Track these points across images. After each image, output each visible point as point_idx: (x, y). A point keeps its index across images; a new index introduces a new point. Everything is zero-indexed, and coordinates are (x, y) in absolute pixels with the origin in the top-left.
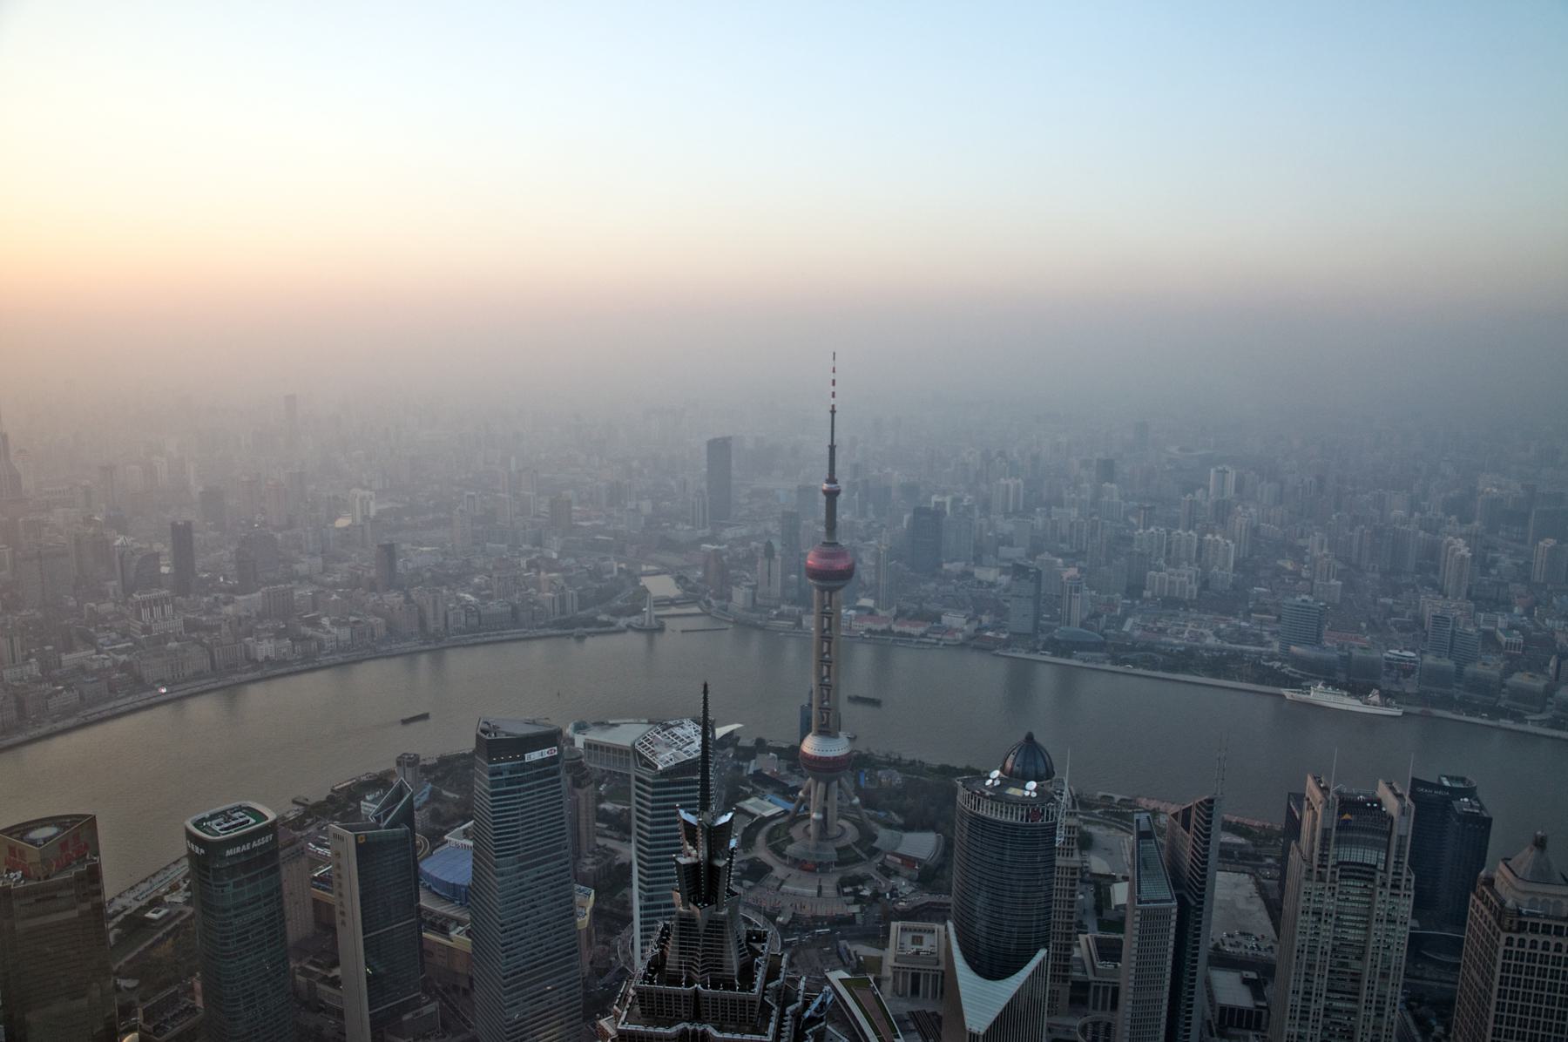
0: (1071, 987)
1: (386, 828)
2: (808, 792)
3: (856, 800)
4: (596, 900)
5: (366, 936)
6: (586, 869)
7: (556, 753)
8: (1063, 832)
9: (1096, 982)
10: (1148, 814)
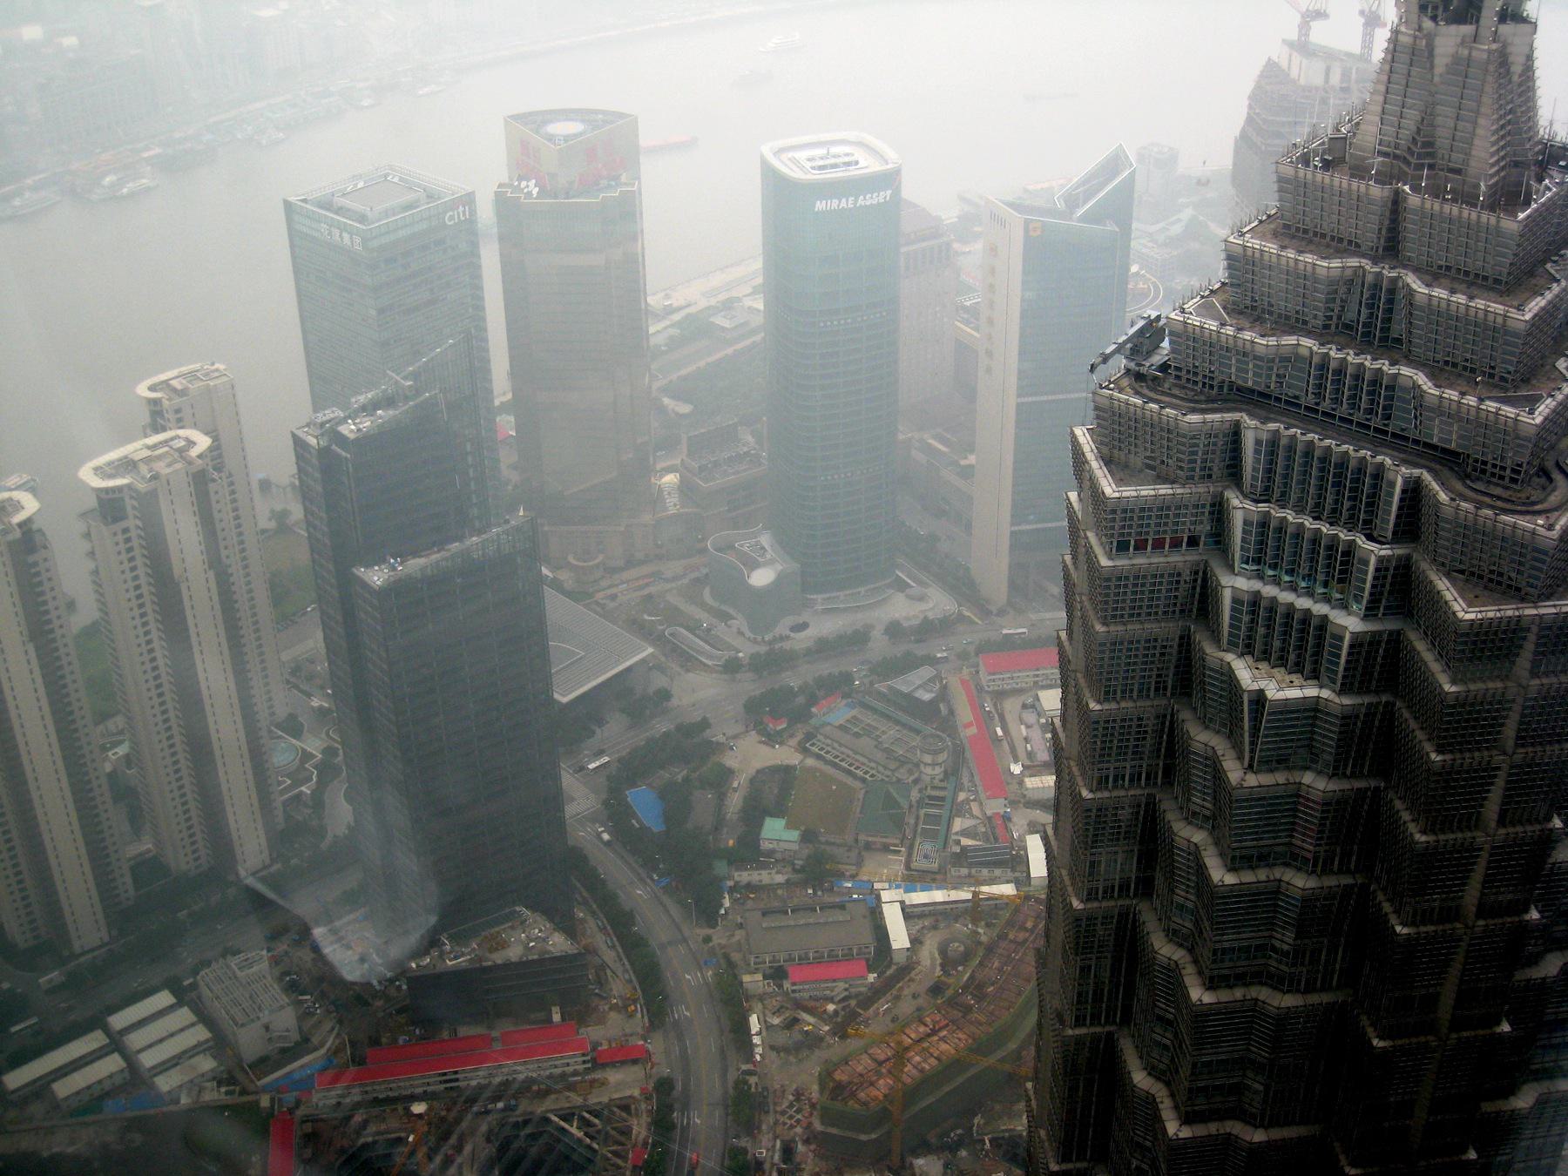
5: (1019, 400)
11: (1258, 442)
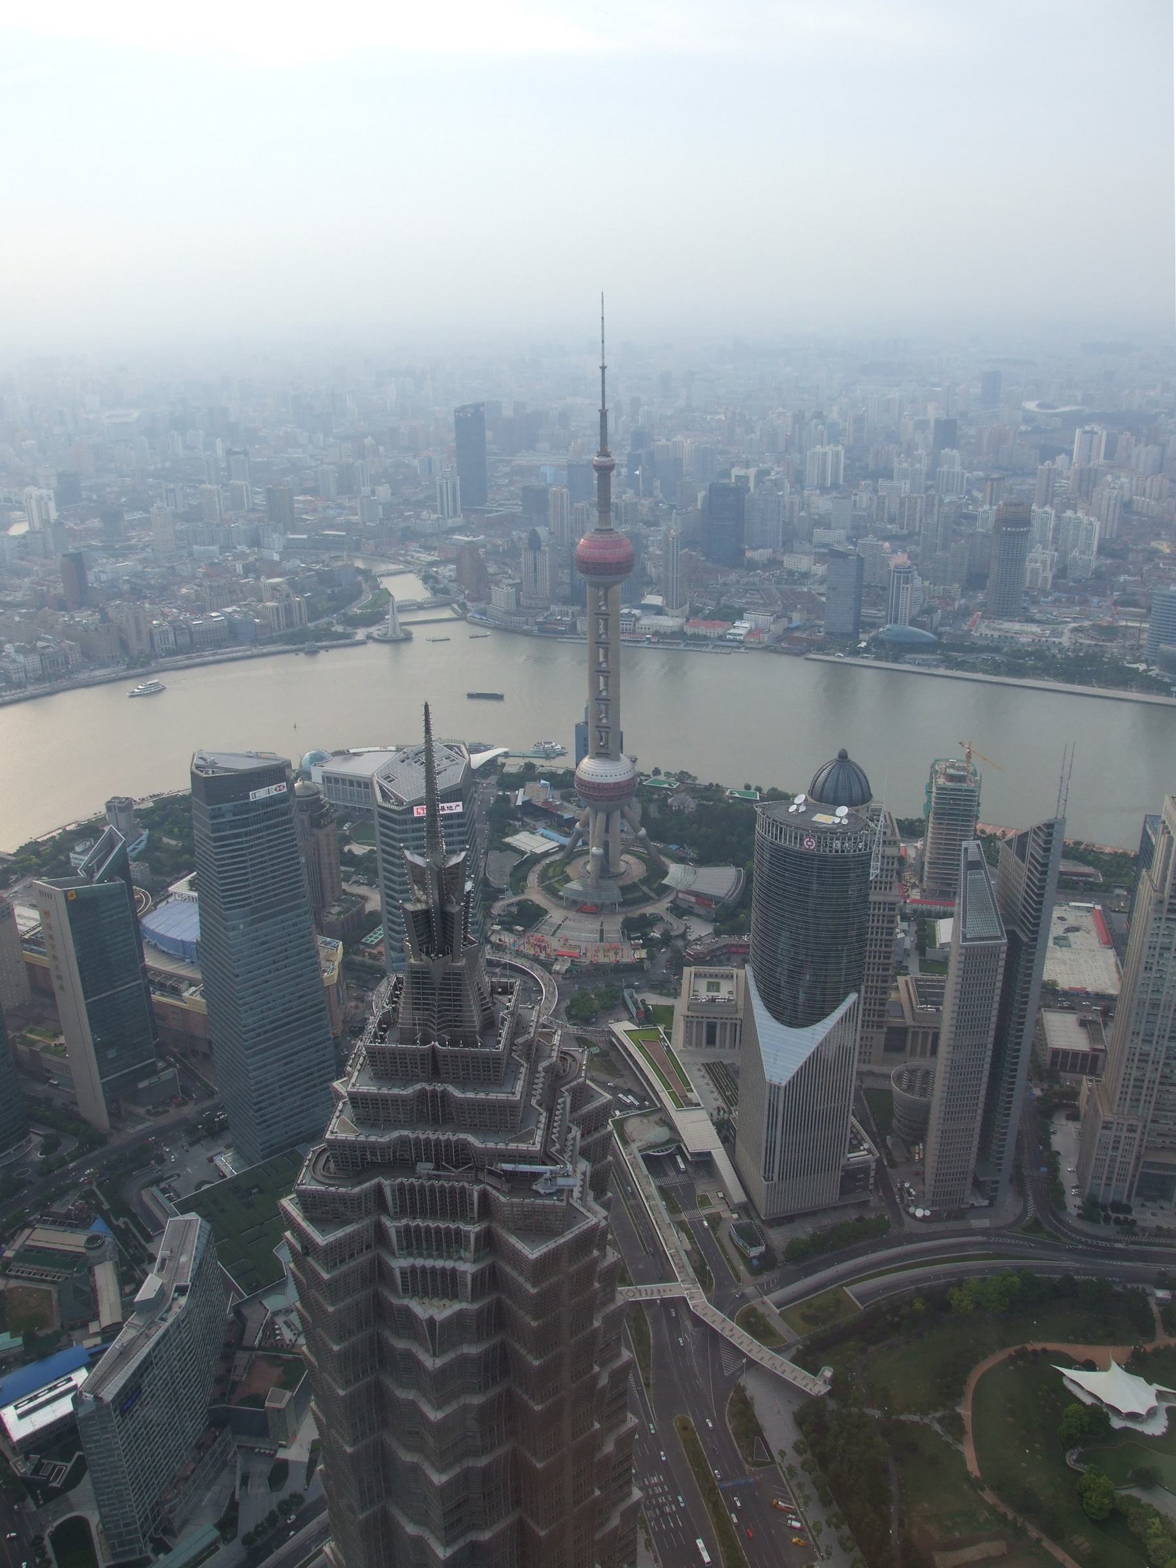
0: (887, 1034)
1: (100, 881)
2: (586, 824)
3: (643, 831)
4: (345, 953)
6: (331, 918)
7: (285, 790)
8: (879, 864)
9: (914, 1027)
10: (979, 842)
11: (393, 1191)
